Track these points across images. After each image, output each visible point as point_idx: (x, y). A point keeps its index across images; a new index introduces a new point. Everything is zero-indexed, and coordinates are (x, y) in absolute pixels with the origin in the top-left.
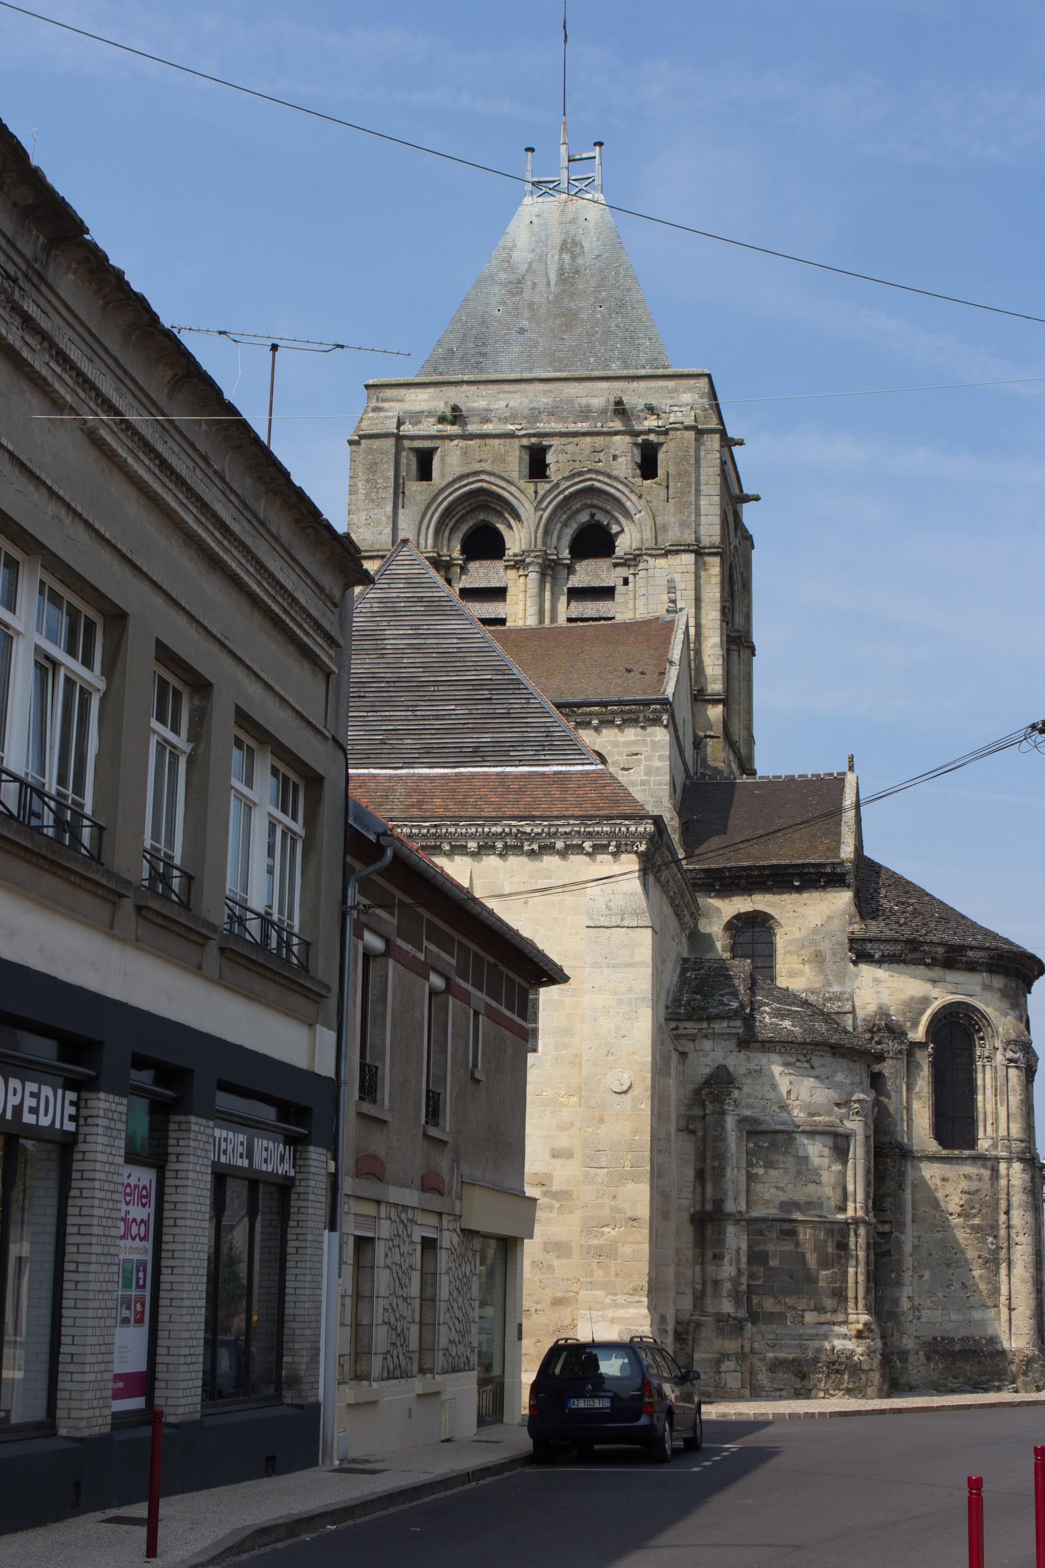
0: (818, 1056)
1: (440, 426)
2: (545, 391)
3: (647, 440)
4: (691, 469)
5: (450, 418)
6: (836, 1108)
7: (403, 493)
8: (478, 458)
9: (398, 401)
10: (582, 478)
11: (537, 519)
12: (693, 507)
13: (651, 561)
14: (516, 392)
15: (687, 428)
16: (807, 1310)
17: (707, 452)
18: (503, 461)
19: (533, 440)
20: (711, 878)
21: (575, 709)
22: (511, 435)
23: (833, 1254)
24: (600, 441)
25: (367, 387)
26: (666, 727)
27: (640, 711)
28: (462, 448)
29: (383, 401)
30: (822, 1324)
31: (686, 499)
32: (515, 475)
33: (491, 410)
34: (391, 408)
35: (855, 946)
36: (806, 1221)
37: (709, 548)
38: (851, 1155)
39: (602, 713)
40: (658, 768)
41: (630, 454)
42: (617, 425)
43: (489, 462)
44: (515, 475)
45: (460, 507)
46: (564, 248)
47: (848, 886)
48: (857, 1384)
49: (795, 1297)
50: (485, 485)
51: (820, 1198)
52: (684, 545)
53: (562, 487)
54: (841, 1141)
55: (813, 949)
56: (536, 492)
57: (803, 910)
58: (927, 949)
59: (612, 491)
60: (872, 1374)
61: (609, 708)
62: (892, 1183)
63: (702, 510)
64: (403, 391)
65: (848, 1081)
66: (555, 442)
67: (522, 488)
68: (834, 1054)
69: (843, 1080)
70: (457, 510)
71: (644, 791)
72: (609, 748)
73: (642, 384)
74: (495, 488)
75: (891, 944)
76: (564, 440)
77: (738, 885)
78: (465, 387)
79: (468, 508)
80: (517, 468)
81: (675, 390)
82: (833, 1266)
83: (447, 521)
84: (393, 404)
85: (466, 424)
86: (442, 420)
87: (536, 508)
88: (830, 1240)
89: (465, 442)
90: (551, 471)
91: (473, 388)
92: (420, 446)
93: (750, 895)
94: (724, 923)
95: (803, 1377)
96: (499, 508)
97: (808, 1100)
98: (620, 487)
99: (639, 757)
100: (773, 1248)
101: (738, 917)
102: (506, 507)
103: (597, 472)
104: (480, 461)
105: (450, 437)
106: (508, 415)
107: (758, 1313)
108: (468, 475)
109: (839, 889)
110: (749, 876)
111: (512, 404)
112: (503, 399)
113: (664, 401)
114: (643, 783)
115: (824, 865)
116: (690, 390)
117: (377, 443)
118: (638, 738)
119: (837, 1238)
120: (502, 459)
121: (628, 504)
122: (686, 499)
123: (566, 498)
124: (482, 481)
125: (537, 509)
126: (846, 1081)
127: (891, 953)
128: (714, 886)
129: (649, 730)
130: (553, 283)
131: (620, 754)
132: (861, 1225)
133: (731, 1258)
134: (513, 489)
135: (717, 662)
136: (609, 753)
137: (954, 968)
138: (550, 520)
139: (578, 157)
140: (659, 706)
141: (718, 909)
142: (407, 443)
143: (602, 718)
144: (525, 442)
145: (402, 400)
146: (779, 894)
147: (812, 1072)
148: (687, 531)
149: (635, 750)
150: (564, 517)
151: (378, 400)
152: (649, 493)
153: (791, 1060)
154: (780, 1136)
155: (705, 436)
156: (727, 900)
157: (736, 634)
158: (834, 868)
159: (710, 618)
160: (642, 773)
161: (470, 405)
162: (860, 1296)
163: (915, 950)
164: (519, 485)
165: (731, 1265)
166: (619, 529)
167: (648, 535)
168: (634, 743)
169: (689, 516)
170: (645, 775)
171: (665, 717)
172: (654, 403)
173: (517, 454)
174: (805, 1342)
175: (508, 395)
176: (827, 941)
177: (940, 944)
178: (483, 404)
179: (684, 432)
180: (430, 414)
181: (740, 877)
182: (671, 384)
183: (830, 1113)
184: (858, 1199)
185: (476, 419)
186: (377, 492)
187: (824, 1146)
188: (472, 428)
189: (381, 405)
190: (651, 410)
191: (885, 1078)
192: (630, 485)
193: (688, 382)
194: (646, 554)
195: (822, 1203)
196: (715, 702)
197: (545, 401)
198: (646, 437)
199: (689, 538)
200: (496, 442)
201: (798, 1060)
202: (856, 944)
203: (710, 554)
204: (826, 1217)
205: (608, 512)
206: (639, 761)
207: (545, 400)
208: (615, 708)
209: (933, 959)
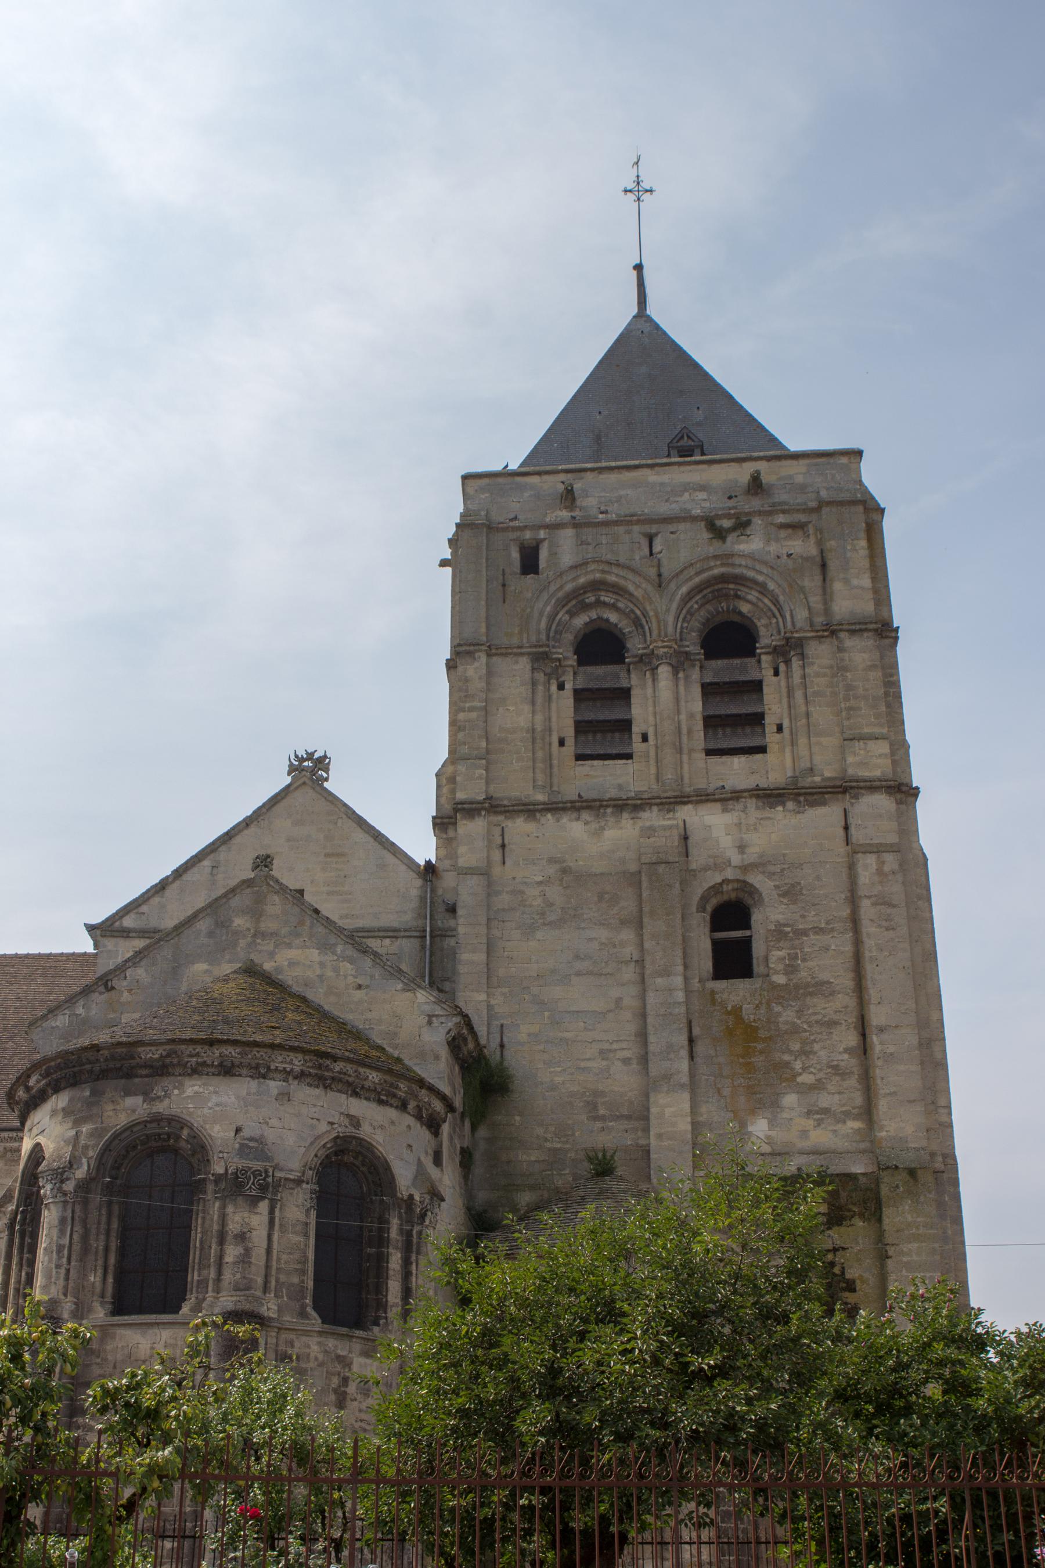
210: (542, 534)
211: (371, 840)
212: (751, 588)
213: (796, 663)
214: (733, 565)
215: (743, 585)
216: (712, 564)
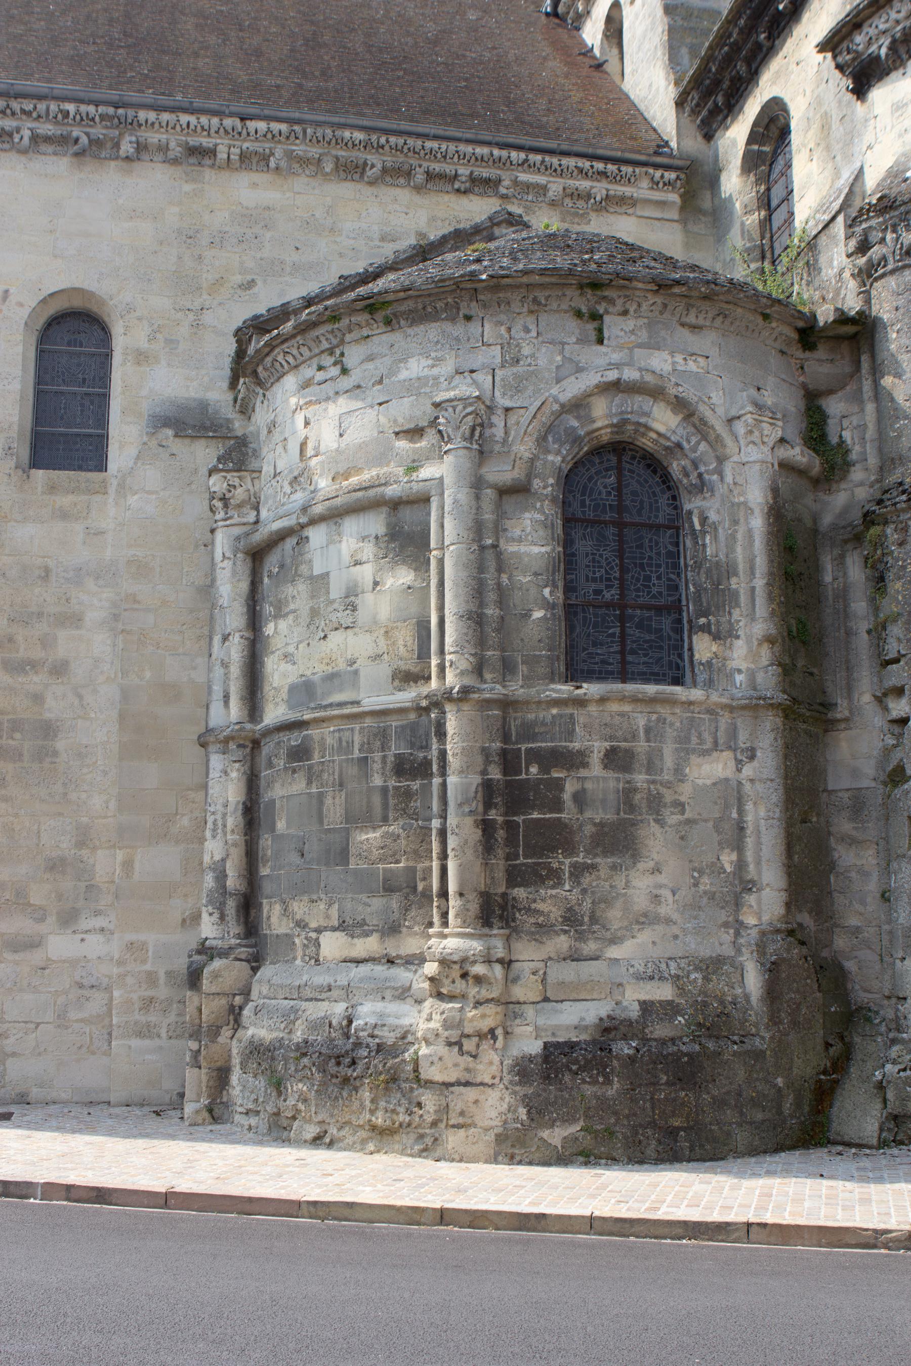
0: (356, 341)
6: (402, 444)
16: (326, 929)
23: (384, 790)
30: (358, 962)
36: (323, 720)
38: (433, 545)
48: (403, 1118)
49: (305, 898)
51: (352, 662)
54: (407, 514)
55: (818, 116)
60: (471, 1094)
62: (898, 585)
65: (447, 368)
68: (388, 322)
69: (426, 372)
82: (385, 819)
88: (378, 756)
95: (278, 1086)
97: (335, 445)
100: (281, 794)
107: (266, 935)
110: (736, 48)
119: (396, 748)
126: (435, 371)
132: (448, 707)
133: (215, 823)
147: (346, 383)
153: (308, 372)
154: (290, 542)
156: (740, 117)
162: (452, 887)
165: (214, 837)
174: (304, 1005)
181: (728, 60)
183: (381, 459)
184: (447, 648)
187: (363, 539)
191: (884, 324)
195: (356, 672)
201: (320, 368)
204: (357, 703)
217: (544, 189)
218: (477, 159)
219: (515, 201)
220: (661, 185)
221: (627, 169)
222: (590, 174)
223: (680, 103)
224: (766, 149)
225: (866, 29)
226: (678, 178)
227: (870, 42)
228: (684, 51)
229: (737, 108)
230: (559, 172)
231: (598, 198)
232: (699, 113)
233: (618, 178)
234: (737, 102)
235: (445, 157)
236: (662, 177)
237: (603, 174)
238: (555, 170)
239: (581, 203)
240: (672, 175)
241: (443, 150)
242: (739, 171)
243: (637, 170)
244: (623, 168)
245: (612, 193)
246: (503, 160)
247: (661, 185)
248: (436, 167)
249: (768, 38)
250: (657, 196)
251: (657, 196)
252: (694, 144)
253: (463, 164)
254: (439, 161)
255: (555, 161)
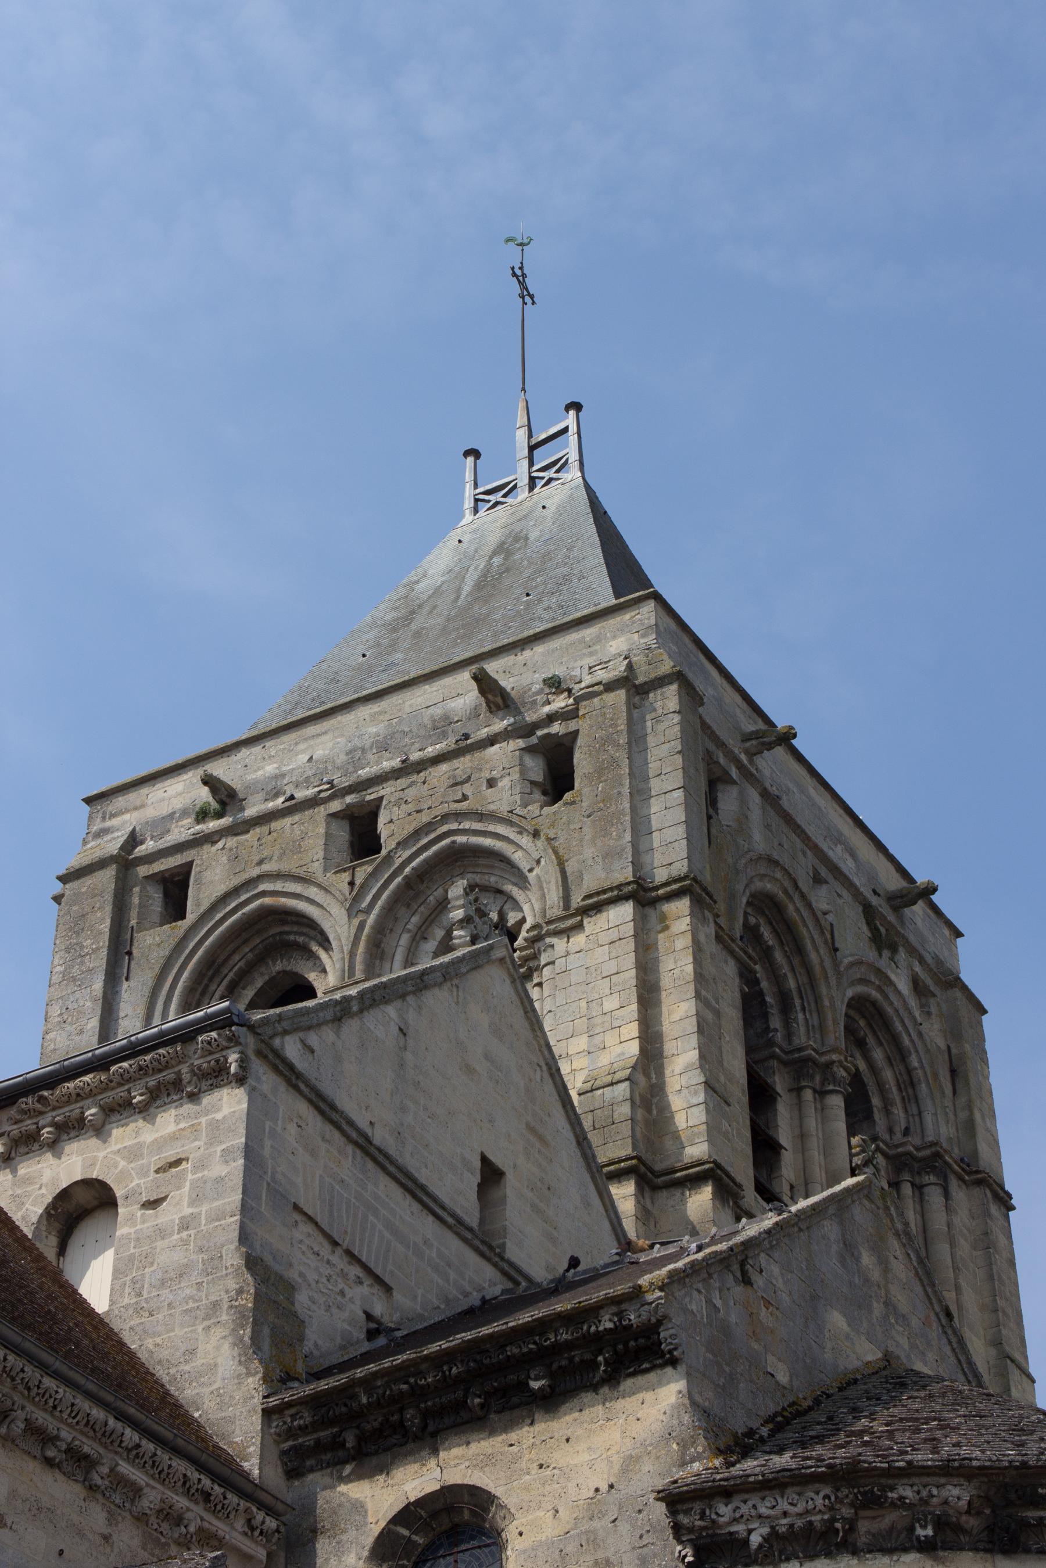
1: (199, 828)
2: (373, 716)
3: (549, 735)
4: (622, 756)
5: (215, 805)
7: (130, 953)
8: (256, 858)
9: (136, 809)
10: (432, 836)
11: (353, 931)
12: (628, 818)
13: (560, 944)
14: (325, 733)
15: (610, 687)
17: (657, 720)
18: (298, 849)
19: (349, 799)
20: (332, 1423)
21: (45, 1093)
22: (313, 802)
24: (463, 764)
25: (89, 801)
26: (241, 1080)
27: (181, 1059)
28: (231, 850)
29: (113, 816)
31: (613, 808)
32: (317, 868)
33: (283, 775)
34: (124, 823)
35: (684, 1520)
37: (666, 884)
39: (104, 1087)
40: (219, 1180)
41: (517, 769)
42: (500, 725)
43: (275, 858)
44: (317, 868)
45: (237, 957)
46: (501, 548)
47: (673, 1362)
50: (267, 901)
52: (611, 889)
53: (398, 862)
56: (351, 884)
57: (563, 1457)
58: (908, 1493)
59: (487, 842)
61: (113, 1068)
63: (653, 823)
64: (144, 791)
66: (387, 790)
67: (325, 884)
70: (231, 962)
71: (185, 1243)
72: (122, 1163)
73: (540, 649)
74: (283, 900)
75: (791, 1493)
76: (402, 782)
77: (400, 1428)
78: (244, 752)
79: (250, 956)
80: (321, 855)
81: (598, 639)
83: (213, 987)
84: (127, 817)
85: (242, 809)
86: (203, 815)
87: (349, 911)
89: (235, 839)
90: (387, 844)
91: (257, 750)
92: (163, 868)
93: (435, 1452)
94: (369, 1541)
96: (301, 939)
98: (501, 829)
99: (184, 1165)
101: (406, 1515)
102: (312, 933)
103: (458, 816)
104: (260, 862)
105: (209, 839)
106: (310, 773)
108: (235, 891)
109: (652, 1376)
110: (419, 1393)
111: (319, 753)
112: (303, 751)
113: (579, 663)
114: (185, 1225)
115: (593, 1311)
116: (622, 630)
117: (88, 881)
118: (182, 1125)
120: (297, 848)
121: (518, 857)
122: (613, 808)
123: (408, 883)
124: (263, 894)
125: (352, 911)
127: (799, 1523)
128: (343, 1445)
129: (207, 1100)
130: (464, 593)
131: (143, 1173)
134: (313, 892)
135: (695, 1100)
136: (124, 1176)
137: (1027, 1551)
138: (381, 930)
139: (543, 436)
140: (214, 1034)
141: (359, 1507)
142: (143, 871)
143: (110, 1097)
144: (336, 806)
145: (143, 806)
146: (506, 1429)
148: (617, 865)
149: (170, 1154)
150: (415, 919)
151: (104, 818)
152: (552, 825)
155: (651, 695)
156: (381, 1478)
157: (927, 1152)
158: (620, 1314)
159: (676, 1017)
160: (185, 1203)
161: (251, 777)
163: (872, 1502)
164: (320, 877)
166: (519, 916)
167: (554, 896)
168: (174, 1137)
169: (620, 837)
170: (191, 1204)
171: (233, 1057)
172: (560, 671)
173: (322, 830)
175: (312, 742)
176: (624, 1527)
177: (949, 1470)
178: (270, 769)
179: (605, 696)
180: (184, 813)
182: (588, 633)
185: (260, 796)
186: (82, 963)
188: (251, 811)
189: (108, 824)
190: (555, 684)
192: (515, 819)
193: (618, 619)
194: (550, 934)
196: (695, 1181)
197: (374, 730)
198: (545, 731)
199: (623, 873)
200: (287, 821)
202: (687, 1512)
203: (670, 897)
205: (500, 892)
206: (182, 1177)
207: (373, 730)
208: (125, 1065)
209: (941, 1523)
210: (734, 773)
211: (574, 1143)
212: (881, 1044)
213: (935, 1197)
214: (886, 997)
215: (875, 1033)
216: (873, 978)
217: (136, 1491)
218: (87, 1424)
219: (100, 1497)
220: (257, 1533)
221: (232, 1498)
222: (192, 1491)
223: (268, 1413)
224: (419, 1539)
225: (736, 1502)
226: (278, 1531)
227: (735, 1520)
228: (266, 1331)
229: (374, 1461)
230: (163, 1476)
231: (192, 1529)
232: (295, 1437)
233: (219, 1507)
234: (376, 1453)
235: (55, 1407)
236: (263, 1523)
237: (207, 1496)
238: (160, 1473)
239: (165, 1527)
240: (271, 1524)
241: (59, 1396)
242: (366, 1553)
243: (242, 1502)
244: (229, 1495)
245: (206, 1525)
246: (114, 1436)
247: (257, 1533)
248: (41, 1417)
249: (482, 1406)
250: (247, 1545)
251: (247, 1545)
252: (275, 1479)
253: (69, 1425)
254: (46, 1410)
255: (164, 1457)
